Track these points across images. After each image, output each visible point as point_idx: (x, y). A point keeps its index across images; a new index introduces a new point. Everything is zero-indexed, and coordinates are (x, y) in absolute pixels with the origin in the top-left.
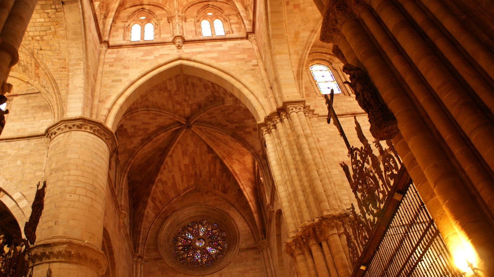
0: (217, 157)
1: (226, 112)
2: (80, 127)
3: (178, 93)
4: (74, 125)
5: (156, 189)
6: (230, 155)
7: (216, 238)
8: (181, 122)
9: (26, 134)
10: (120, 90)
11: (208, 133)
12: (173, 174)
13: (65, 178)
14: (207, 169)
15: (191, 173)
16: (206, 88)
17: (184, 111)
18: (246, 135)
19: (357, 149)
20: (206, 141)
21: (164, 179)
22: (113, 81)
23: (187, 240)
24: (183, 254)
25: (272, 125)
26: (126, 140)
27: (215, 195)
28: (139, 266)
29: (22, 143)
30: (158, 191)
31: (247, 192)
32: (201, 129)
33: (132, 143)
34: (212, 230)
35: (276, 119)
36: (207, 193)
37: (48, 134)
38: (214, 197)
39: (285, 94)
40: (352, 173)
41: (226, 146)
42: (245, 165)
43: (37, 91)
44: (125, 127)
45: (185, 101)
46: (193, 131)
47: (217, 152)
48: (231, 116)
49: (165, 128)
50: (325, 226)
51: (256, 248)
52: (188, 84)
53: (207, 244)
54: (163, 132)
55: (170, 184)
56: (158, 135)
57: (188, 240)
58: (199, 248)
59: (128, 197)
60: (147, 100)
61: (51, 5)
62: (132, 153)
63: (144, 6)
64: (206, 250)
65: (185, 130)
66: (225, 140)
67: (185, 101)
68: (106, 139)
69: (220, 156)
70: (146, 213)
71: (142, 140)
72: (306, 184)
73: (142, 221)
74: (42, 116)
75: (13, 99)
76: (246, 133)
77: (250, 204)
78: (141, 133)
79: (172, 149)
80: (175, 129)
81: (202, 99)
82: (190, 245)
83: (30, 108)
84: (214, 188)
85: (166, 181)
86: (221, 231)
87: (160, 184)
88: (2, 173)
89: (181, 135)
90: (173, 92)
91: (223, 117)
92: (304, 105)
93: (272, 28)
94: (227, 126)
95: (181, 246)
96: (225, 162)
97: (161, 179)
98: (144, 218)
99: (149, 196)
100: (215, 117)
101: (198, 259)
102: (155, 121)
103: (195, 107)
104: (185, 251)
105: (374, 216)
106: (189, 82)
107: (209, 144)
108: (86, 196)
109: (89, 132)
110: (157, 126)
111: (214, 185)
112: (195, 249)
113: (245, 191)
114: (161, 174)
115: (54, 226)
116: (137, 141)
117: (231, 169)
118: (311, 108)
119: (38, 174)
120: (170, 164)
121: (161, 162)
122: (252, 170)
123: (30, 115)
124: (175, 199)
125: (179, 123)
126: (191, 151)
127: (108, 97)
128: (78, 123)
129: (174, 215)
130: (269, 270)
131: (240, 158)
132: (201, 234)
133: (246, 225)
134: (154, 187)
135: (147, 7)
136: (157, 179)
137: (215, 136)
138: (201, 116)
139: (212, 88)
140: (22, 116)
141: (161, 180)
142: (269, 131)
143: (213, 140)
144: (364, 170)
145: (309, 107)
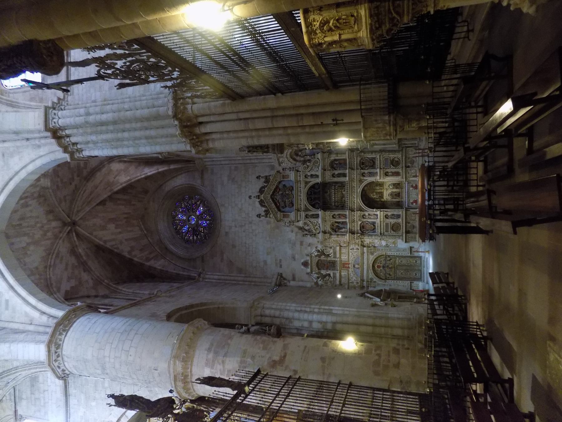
0: (110, 197)
1: (60, 185)
2: (58, 346)
3: (31, 234)
4: (56, 352)
5: (138, 257)
7: (190, 205)
8: (67, 231)
9: (63, 399)
10: (19, 301)
13: (112, 361)
14: (122, 207)
16: (27, 206)
17: (54, 228)
19: (99, 71)
21: (129, 249)
22: (7, 308)
23: (188, 231)
24: (201, 236)
25: (73, 146)
28: (207, 276)
31: (149, 171)
32: (78, 211)
33: (87, 281)
34: (182, 208)
35: (66, 142)
36: (146, 209)
37: (64, 377)
39: (35, 126)
40: (128, 81)
43: (12, 390)
44: (69, 289)
45: (42, 227)
46: (80, 219)
47: (105, 196)
49: (74, 247)
50: (182, 116)
51: (202, 171)
53: (194, 214)
54: (78, 249)
56: (80, 254)
57: (188, 231)
58: (197, 221)
59: (144, 284)
60: (37, 268)
62: (98, 282)
64: (199, 215)
65: (77, 227)
68: (75, 317)
69: (109, 194)
70: (159, 268)
71: (84, 271)
72: (139, 125)
73: (167, 271)
74: (43, 384)
75: (20, 415)
76: (85, 167)
77: (160, 170)
80: (75, 239)
82: (193, 229)
83: (33, 396)
86: (184, 199)
87: (133, 253)
88: (103, 420)
89: (83, 231)
90: (30, 241)
92: (50, 108)
94: (76, 185)
95: (193, 237)
96: (116, 190)
98: (164, 269)
99: (144, 264)
100: (65, 197)
101: (206, 223)
103: (51, 217)
104: (198, 235)
105: (175, 71)
106: (18, 223)
107: (95, 204)
108: (132, 341)
109: (65, 336)
112: (197, 225)
115: (159, 371)
116: (85, 276)
117: (124, 185)
118: (56, 100)
119: (106, 385)
120: (113, 243)
121: (111, 252)
122: (126, 164)
123: (42, 395)
125: (69, 232)
127: (26, 314)
128: (53, 349)
130: (223, 163)
132: (185, 218)
133: (180, 177)
134: (135, 259)
136: (128, 256)
140: (42, 404)
141: (129, 252)
142: (80, 151)
144: (123, 69)
145: (53, 103)
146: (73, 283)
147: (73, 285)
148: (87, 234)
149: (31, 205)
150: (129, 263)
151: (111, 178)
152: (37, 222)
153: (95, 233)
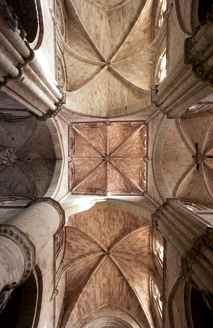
0: (124, 279)
1: (132, 243)
3: (105, 225)
6: (133, 278)
11: (120, 261)
12: (95, 289)
15: (107, 291)
16: (120, 222)
17: (107, 241)
18: (144, 258)
20: (118, 266)
21: (88, 292)
26: (70, 253)
27: (122, 310)
29: (12, 209)
30: (83, 301)
32: (115, 258)
33: (73, 255)
38: (121, 313)
41: (130, 271)
42: (143, 288)
44: (71, 245)
47: (125, 275)
49: (94, 252)
52: (110, 219)
55: (92, 297)
60: (87, 224)
61: (50, 162)
63: (93, 190)
67: (108, 233)
69: (127, 278)
70: (72, 314)
73: (67, 320)
78: (80, 251)
79: (97, 269)
81: (118, 232)
84: (122, 305)
85: (89, 293)
87: (85, 295)
90: (102, 224)
93: (157, 176)
94: (131, 254)
96: (129, 282)
97: (86, 291)
99: (76, 301)
100: (124, 248)
106: (112, 218)
110: (90, 250)
111: (121, 302)
113: (143, 306)
114: (87, 287)
120: (94, 281)
121: (88, 278)
122: (147, 292)
124: (93, 311)
125: (103, 250)
126: (108, 273)
129: (91, 322)
131: (139, 281)
134: (81, 295)
135: (94, 190)
138: (116, 247)
139: (123, 221)
141: (86, 292)
143: (122, 267)
146: (74, 248)
147: (73, 248)
148: (101, 262)
149: (120, 224)
150: (79, 290)
151: (136, 280)
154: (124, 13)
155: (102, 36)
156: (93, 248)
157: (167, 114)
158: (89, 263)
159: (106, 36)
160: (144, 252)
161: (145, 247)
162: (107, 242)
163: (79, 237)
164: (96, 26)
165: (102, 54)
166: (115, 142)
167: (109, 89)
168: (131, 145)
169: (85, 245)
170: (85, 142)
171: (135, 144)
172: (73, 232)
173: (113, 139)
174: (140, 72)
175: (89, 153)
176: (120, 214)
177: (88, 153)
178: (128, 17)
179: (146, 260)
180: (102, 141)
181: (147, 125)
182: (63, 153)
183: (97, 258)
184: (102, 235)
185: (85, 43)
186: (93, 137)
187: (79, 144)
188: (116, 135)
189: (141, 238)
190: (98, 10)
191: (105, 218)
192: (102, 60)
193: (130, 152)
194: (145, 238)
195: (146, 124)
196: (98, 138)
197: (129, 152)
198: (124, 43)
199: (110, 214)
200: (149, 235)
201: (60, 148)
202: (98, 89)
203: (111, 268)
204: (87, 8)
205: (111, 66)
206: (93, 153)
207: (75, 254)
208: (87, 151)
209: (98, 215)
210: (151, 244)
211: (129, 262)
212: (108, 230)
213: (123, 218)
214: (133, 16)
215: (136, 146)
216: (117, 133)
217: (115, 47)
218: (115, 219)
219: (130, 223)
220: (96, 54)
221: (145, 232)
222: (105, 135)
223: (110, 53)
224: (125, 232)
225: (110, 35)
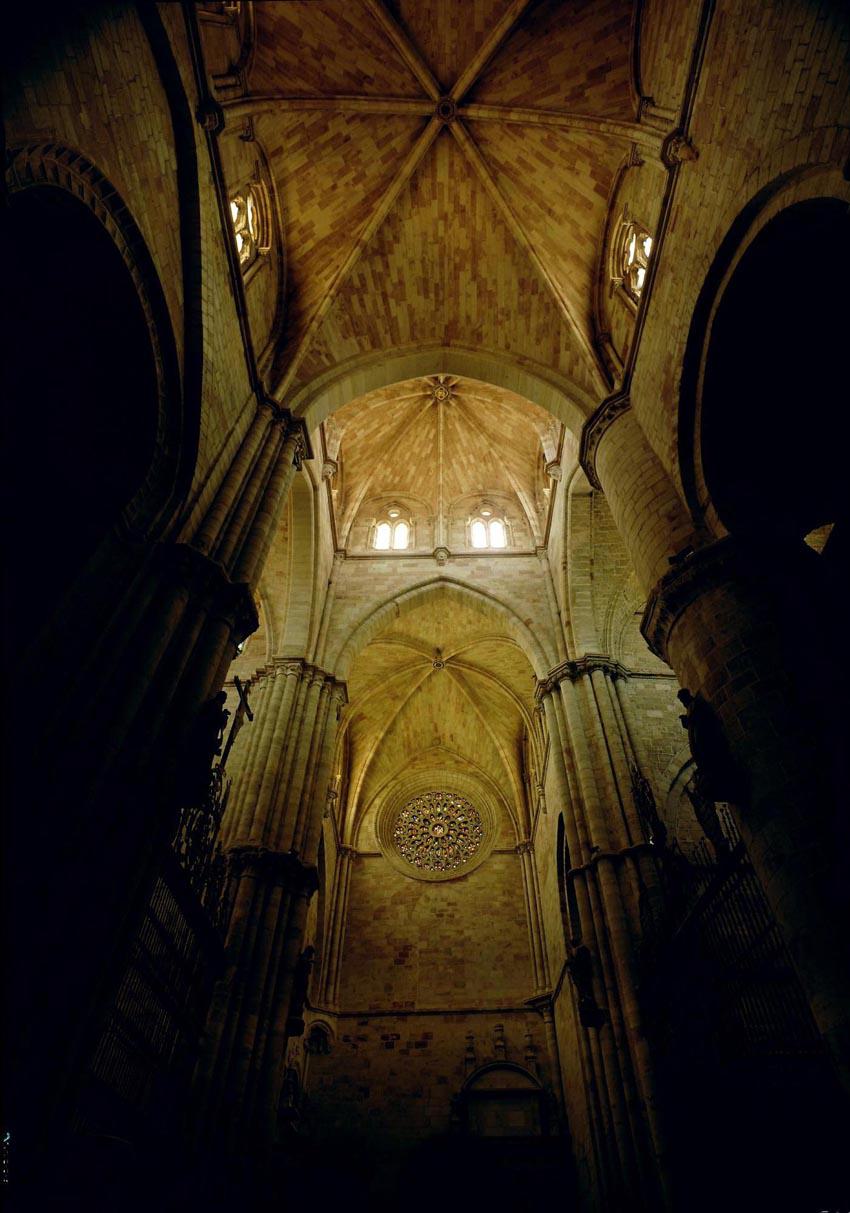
1: (352, 175)
16: (401, 283)
17: (452, 174)
26: (603, 156)
44: (593, 183)
45: (444, 217)
48: (340, 160)
52: (437, 285)
66: (350, 48)
90: (468, 266)
91: (359, 152)
100: (379, 145)
102: (523, 155)
103: (425, 185)
106: (432, 295)
110: (522, 136)
137: (378, 59)
139: (389, 289)
146: (584, 167)
149: (400, 271)
152: (435, 235)
153: (479, 24)
154: (407, 745)
155: (453, 709)
156: (506, 138)
157: (305, 666)
158: (531, 58)
159: (443, 707)
160: (301, 150)
161: (296, 172)
162: (452, 164)
163: (558, 209)
164: (464, 725)
165: (454, 681)
166: (419, 445)
167: (439, 623)
168: (370, 442)
169: (538, 162)
170: (509, 453)
171: (359, 446)
172: (578, 237)
173: (426, 459)
174: (366, 654)
175: (499, 418)
176: (403, 323)
177: (502, 416)
178: (400, 741)
179: (286, 125)
180: (457, 452)
181: (337, 550)
182: (569, 511)
183: (496, 80)
184: (468, 207)
185: (489, 699)
186: (482, 465)
187: (526, 448)
188: (416, 472)
189: (317, 206)
190: (458, 748)
191: (455, 294)
192: (451, 670)
193: (373, 421)
194: (302, 211)
195: (340, 551)
196: (469, 461)
197: (377, 420)
198: (406, 699)
199: (437, 310)
200: (288, 231)
201: (573, 531)
202: (464, 627)
203: (434, 24)
204: (480, 756)
205: (433, 660)
206: (486, 412)
207: (586, 146)
208: (506, 425)
209: (480, 313)
210: (277, 198)
211: (353, 71)
212: (446, 231)
213: (392, 302)
214: (389, 743)
215: (356, 440)
216: (413, 477)
217: (424, 689)
218: (419, 293)
219: (366, 292)
220: (466, 678)
221: (304, 241)
222: (450, 472)
223: (434, 679)
224: (380, 232)
225: (436, 708)
